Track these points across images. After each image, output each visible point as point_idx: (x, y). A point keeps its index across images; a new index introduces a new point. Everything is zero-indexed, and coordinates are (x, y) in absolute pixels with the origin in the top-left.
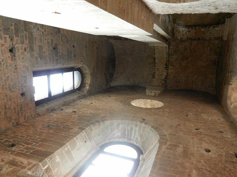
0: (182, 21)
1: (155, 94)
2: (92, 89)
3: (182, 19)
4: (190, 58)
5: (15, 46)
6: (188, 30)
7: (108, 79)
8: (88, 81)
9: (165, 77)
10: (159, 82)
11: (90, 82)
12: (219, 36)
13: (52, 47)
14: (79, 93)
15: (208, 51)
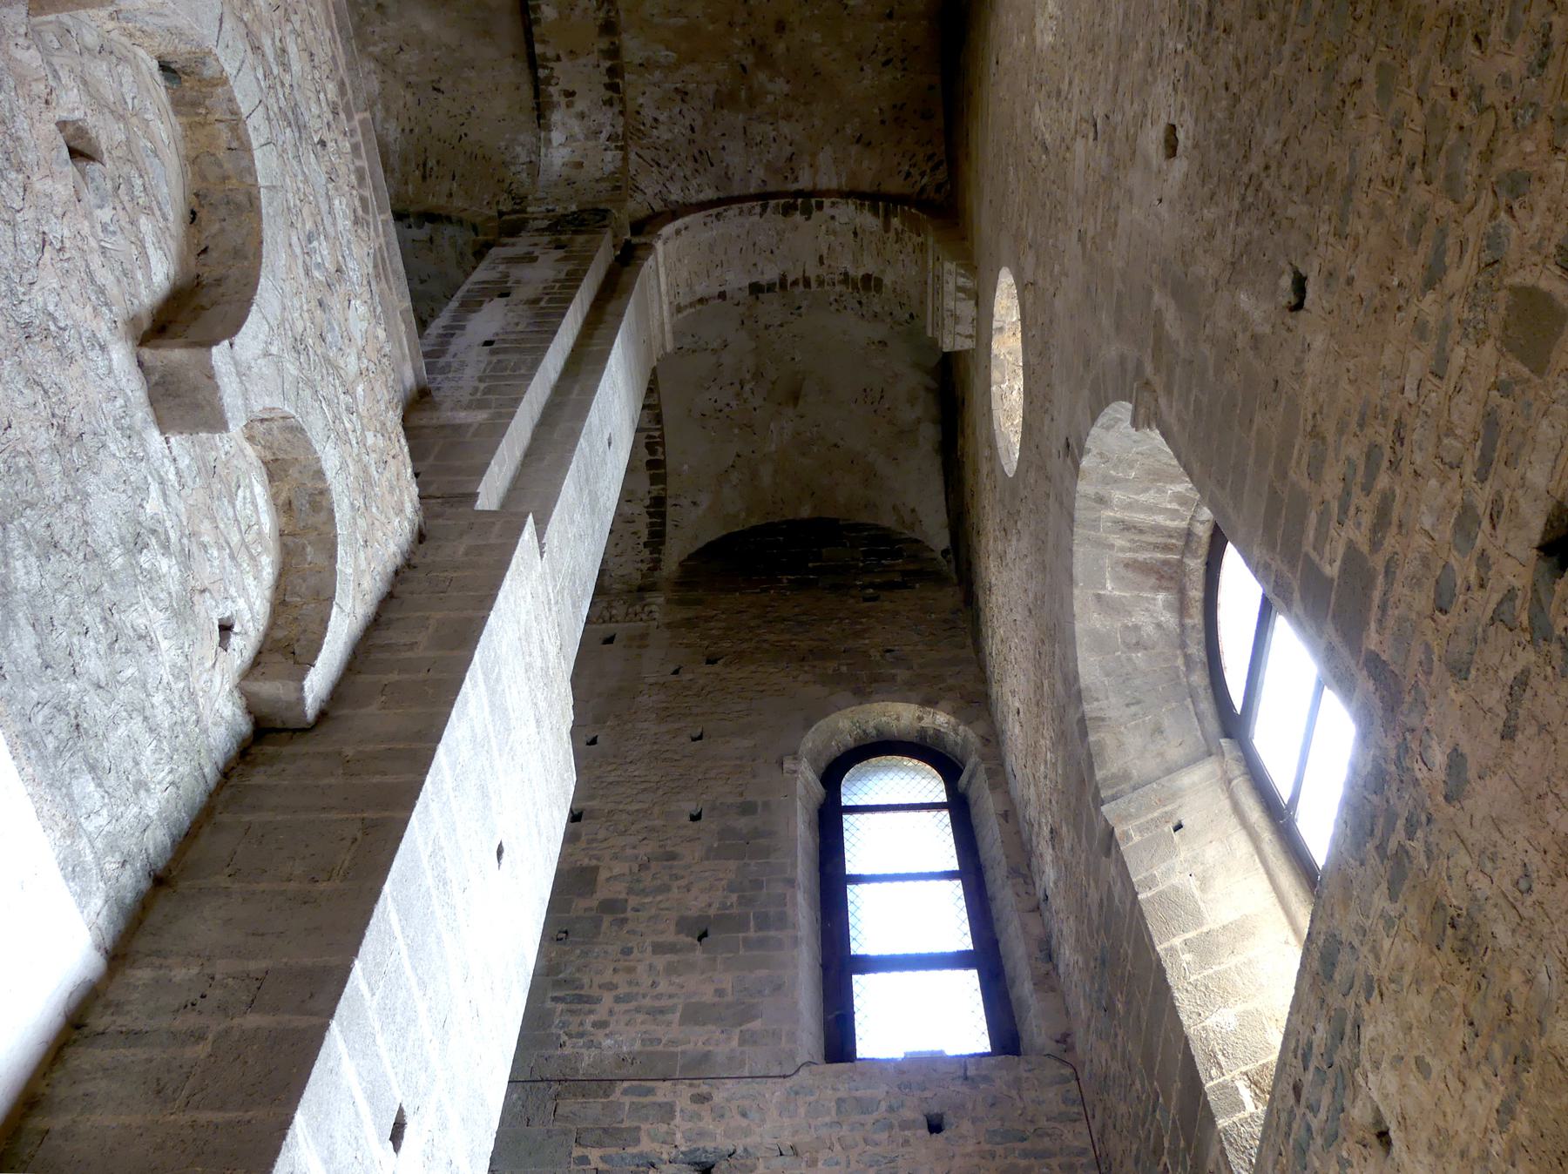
0: (519, 149)
1: (962, 295)
2: (950, 689)
3: (503, 144)
5: (683, 1149)
7: (904, 573)
8: (902, 715)
9: (866, 212)
10: (897, 246)
11: (907, 700)
13: (692, 949)
14: (971, 777)
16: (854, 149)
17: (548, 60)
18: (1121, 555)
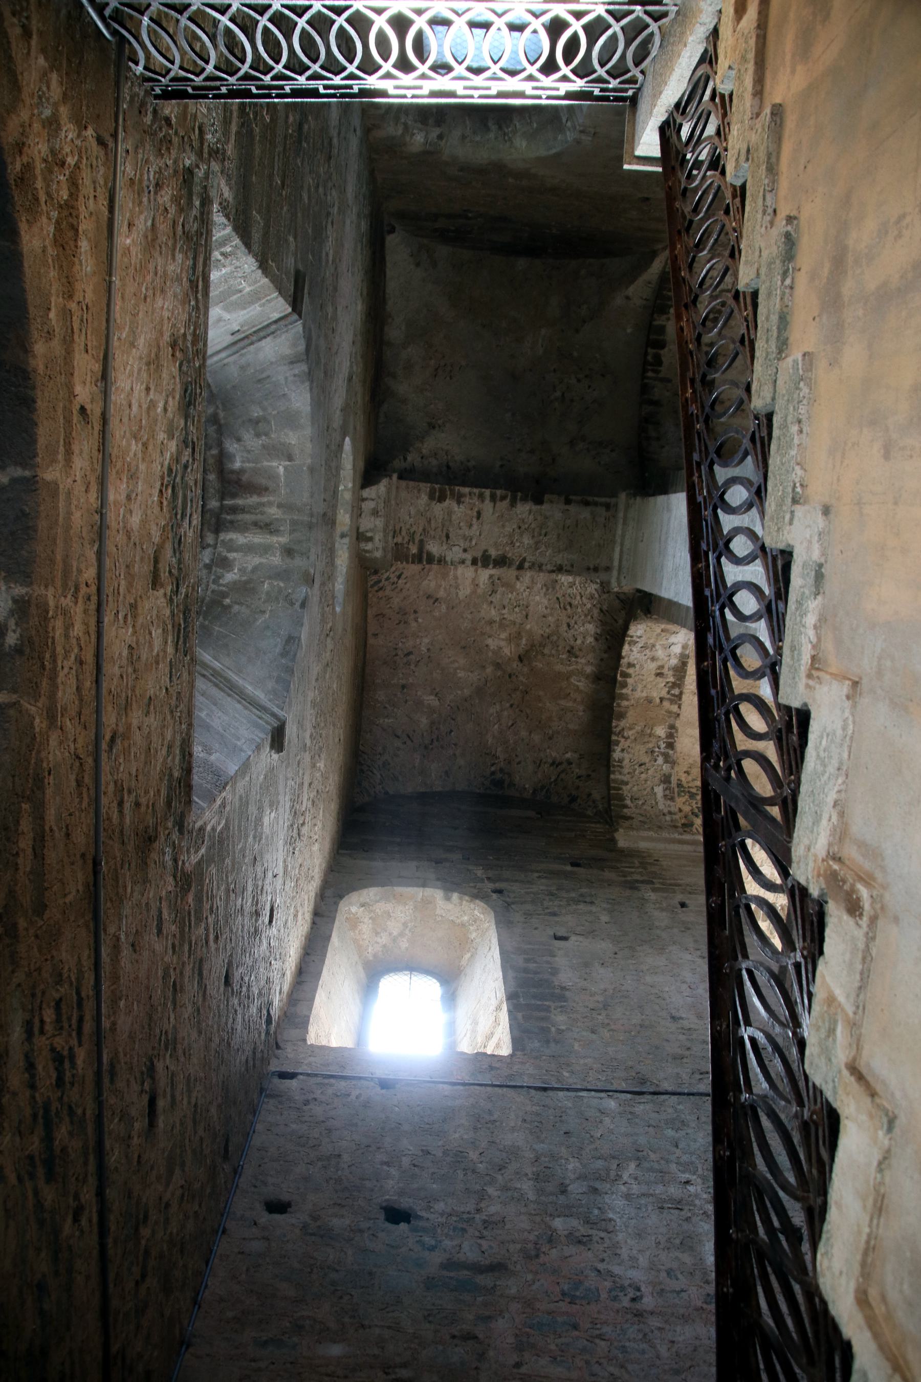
1: (369, 534)
4: (526, 669)
6: (666, 667)
12: (628, 802)
15: (554, 754)
16: (441, 594)
17: (669, 699)
18: (271, 498)
